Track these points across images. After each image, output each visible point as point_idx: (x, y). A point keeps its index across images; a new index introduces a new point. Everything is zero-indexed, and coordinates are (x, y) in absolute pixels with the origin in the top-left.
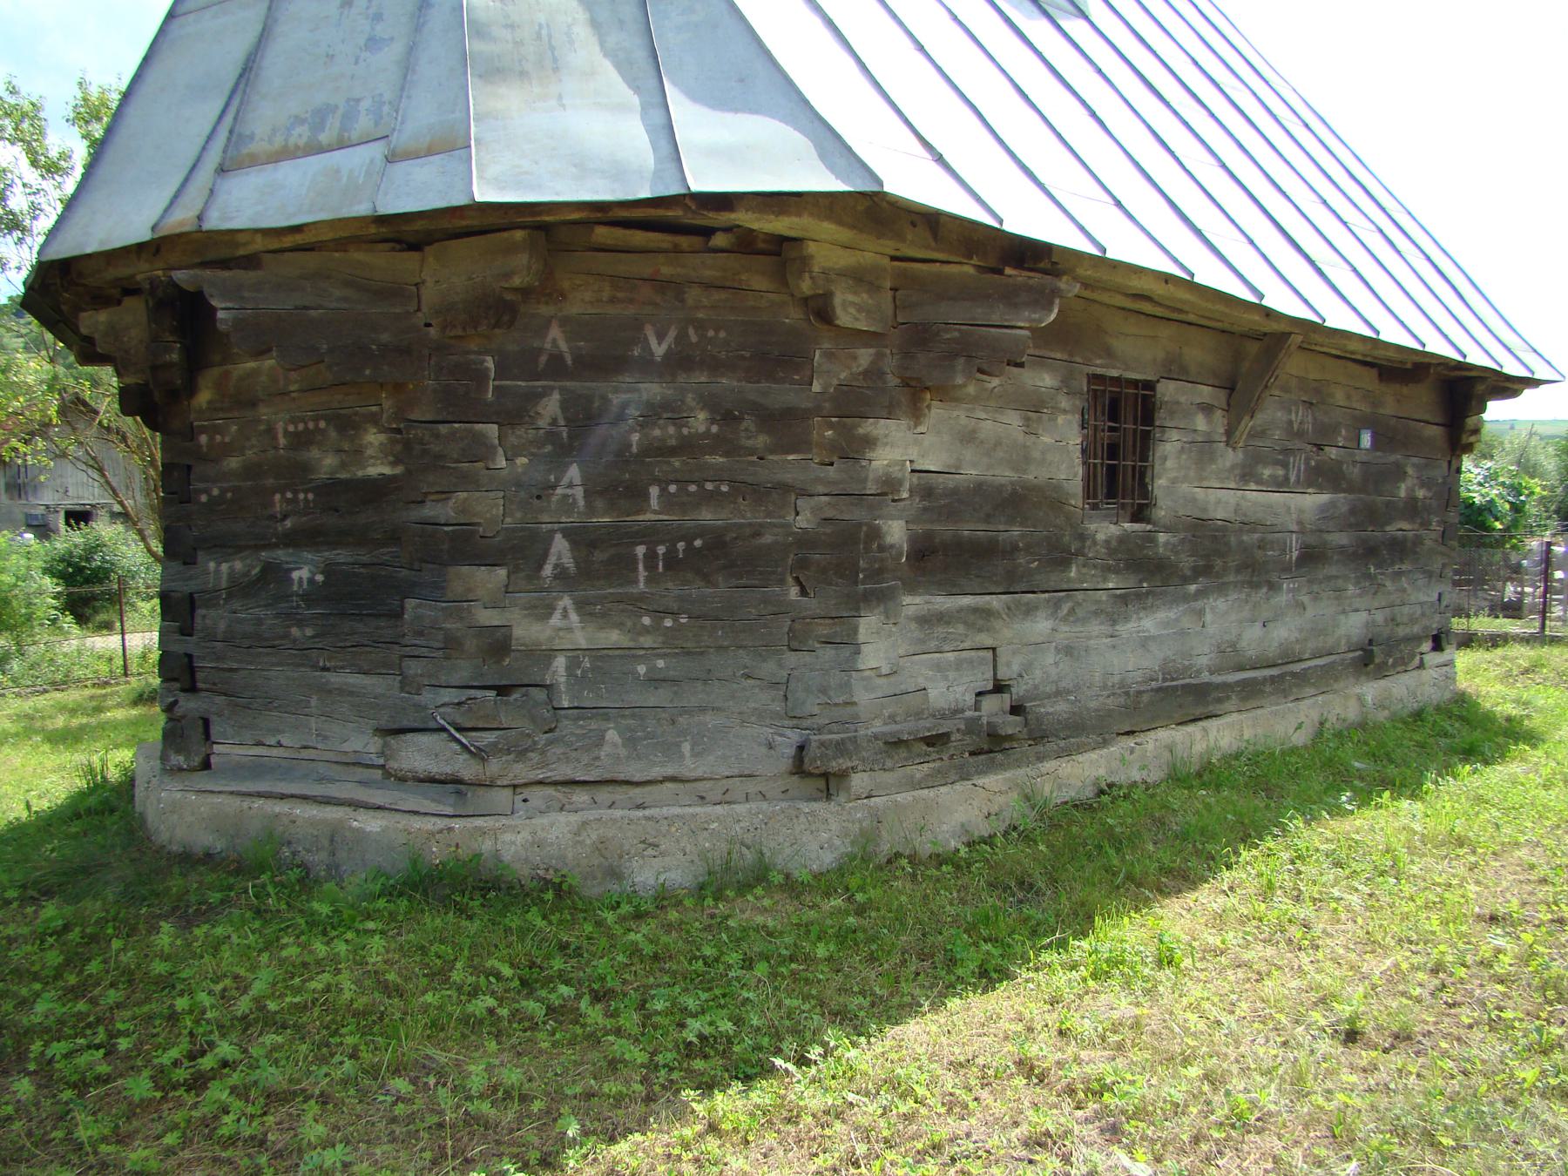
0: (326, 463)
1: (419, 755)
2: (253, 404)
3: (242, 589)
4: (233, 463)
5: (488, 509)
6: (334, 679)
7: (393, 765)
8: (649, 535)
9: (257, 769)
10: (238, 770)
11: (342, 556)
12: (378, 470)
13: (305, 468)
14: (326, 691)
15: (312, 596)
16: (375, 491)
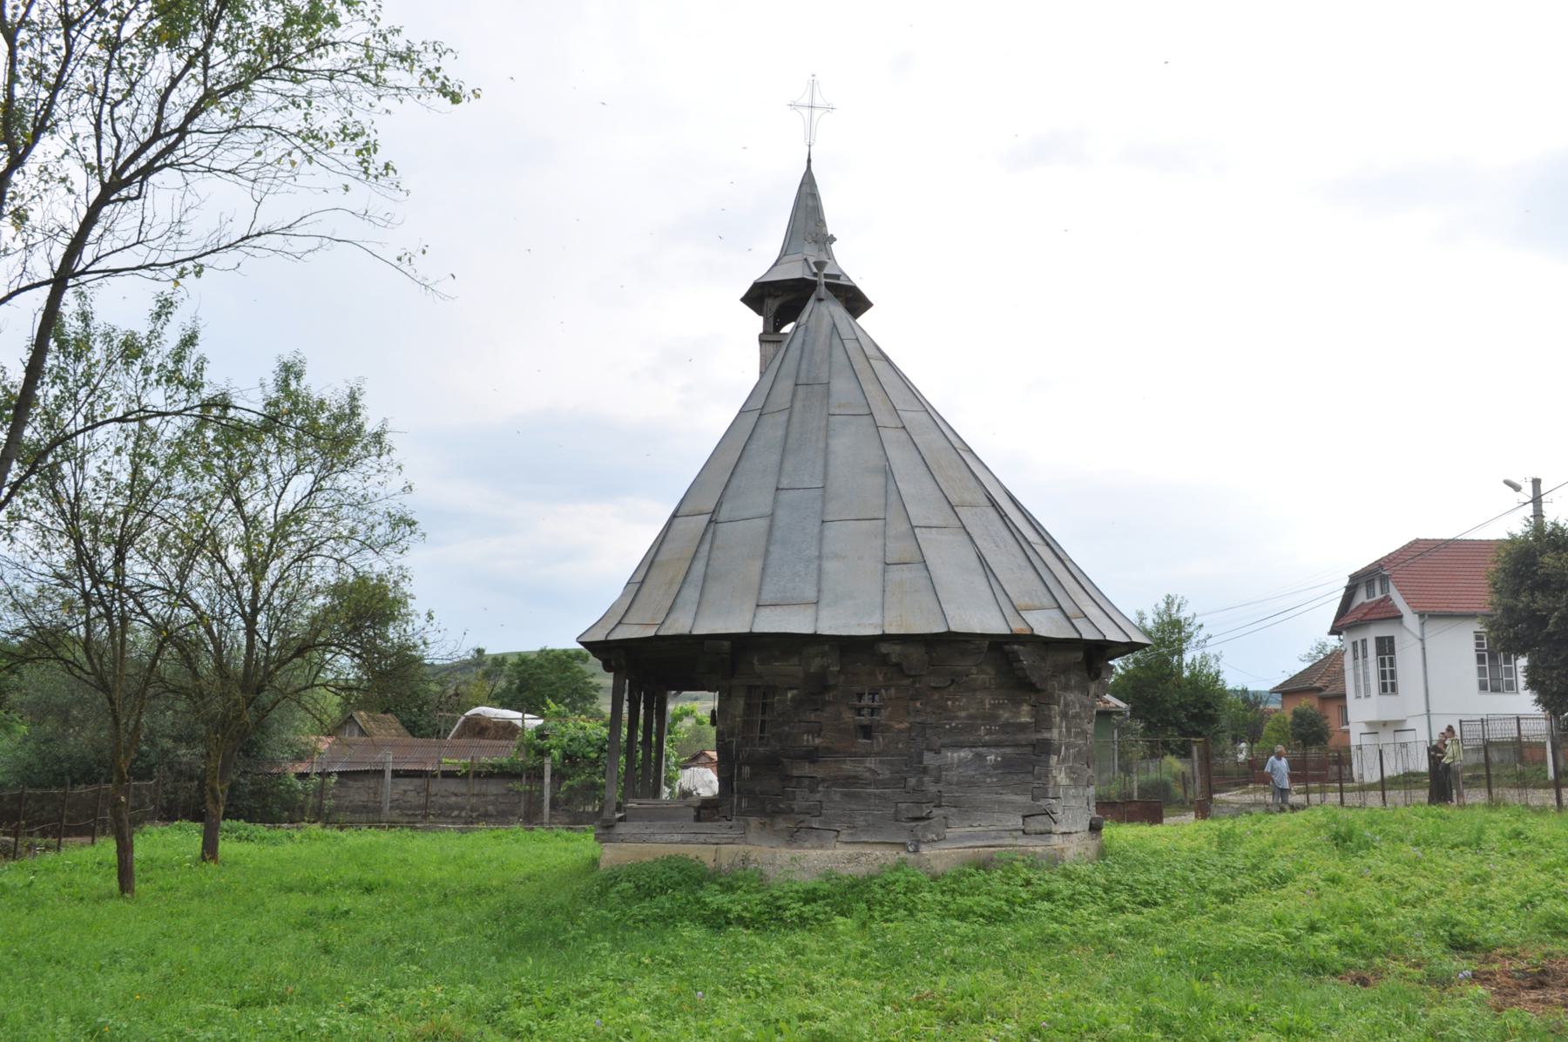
0: (1005, 715)
1: (1035, 824)
2: (975, 690)
3: (962, 763)
4: (963, 714)
5: (1055, 734)
6: (1005, 798)
7: (1028, 829)
8: (1074, 746)
9: (972, 837)
10: (962, 838)
11: (1008, 750)
12: (1025, 719)
13: (996, 717)
14: (1001, 803)
15: (996, 766)
16: (1023, 727)
